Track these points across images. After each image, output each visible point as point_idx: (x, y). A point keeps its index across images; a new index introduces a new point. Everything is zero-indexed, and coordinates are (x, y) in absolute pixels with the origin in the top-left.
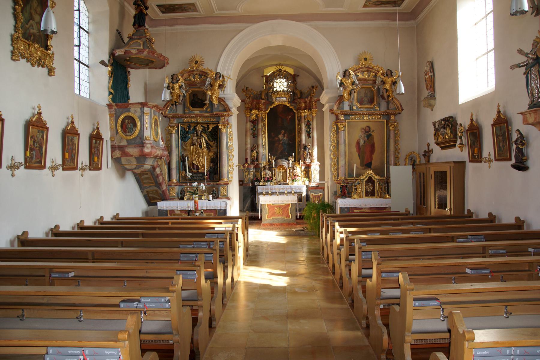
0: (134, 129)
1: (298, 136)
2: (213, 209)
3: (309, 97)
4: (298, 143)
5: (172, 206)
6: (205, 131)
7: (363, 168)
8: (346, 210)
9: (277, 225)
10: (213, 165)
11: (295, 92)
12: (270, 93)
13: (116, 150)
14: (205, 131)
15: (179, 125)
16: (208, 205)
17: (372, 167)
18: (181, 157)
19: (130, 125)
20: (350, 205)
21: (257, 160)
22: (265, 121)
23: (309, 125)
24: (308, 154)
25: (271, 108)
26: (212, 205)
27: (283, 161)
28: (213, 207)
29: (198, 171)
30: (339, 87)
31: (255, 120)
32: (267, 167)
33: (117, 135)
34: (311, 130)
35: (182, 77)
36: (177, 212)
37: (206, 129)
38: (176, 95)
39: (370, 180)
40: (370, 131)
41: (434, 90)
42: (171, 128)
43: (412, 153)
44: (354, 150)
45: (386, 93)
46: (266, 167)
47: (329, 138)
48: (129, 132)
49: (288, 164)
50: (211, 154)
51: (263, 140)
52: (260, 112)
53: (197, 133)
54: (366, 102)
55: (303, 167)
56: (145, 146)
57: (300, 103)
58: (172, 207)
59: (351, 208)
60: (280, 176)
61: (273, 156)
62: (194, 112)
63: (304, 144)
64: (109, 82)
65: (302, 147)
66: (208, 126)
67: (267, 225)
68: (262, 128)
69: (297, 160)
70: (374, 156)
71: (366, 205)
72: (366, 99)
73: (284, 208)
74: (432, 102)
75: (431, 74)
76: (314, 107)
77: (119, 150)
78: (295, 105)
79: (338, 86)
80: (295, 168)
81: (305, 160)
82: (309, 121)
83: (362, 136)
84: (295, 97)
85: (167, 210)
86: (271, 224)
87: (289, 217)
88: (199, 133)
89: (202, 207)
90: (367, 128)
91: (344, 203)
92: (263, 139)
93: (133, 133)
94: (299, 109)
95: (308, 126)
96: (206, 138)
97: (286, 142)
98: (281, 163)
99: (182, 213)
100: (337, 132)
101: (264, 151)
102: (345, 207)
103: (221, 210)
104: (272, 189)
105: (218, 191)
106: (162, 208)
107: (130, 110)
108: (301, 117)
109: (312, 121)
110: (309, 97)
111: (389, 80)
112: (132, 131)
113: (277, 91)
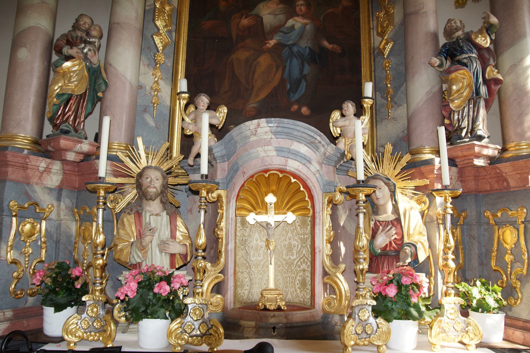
46: (145, 182)
61: (210, 94)
97: (305, 44)
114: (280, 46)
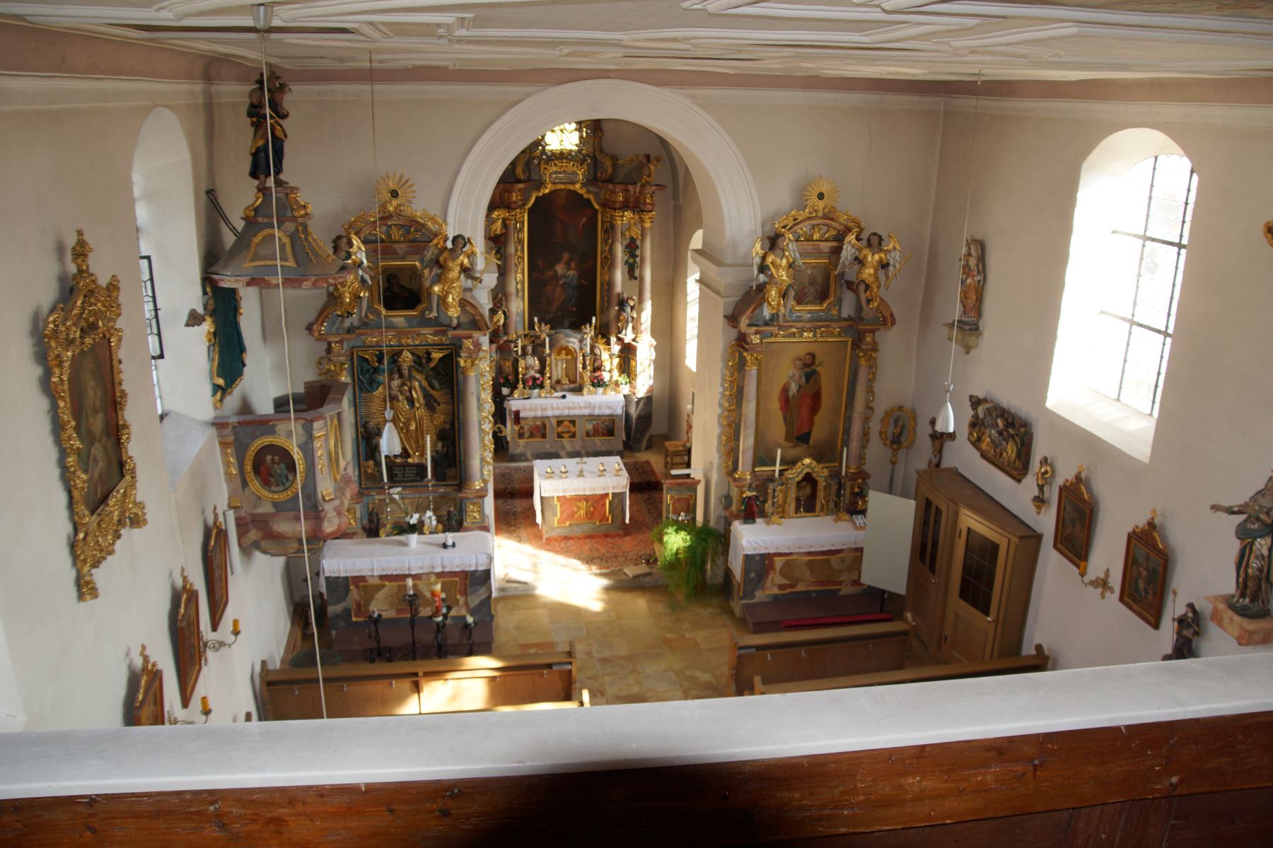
0: (291, 477)
1: (603, 267)
2: (458, 570)
3: (639, 185)
4: (601, 284)
5: (358, 566)
6: (421, 364)
7: (791, 444)
8: (757, 558)
9: (579, 539)
10: (443, 446)
11: (599, 158)
12: (534, 158)
13: (248, 531)
14: (421, 364)
15: (352, 354)
16: (446, 563)
17: (811, 442)
18: (362, 430)
19: (280, 468)
20: (766, 548)
21: (506, 333)
22: (521, 230)
23: (632, 248)
24: (630, 319)
25: (537, 198)
26: (457, 562)
27: (567, 336)
28: (457, 566)
29: (406, 462)
30: (758, 275)
31: (500, 236)
32: (530, 348)
33: (247, 489)
34: (638, 260)
35: (357, 234)
36: (372, 581)
37: (424, 361)
38: (350, 293)
39: (809, 479)
40: (813, 364)
41: (979, 314)
42: (335, 366)
43: (900, 408)
44: (775, 405)
45: (865, 292)
47: (720, 376)
48: (277, 485)
49: (581, 341)
50: (440, 418)
51: (519, 278)
52: (514, 213)
53: (400, 371)
54: (811, 298)
55: (616, 348)
56: (324, 519)
57: (613, 192)
58: (359, 571)
59: (769, 554)
60: (559, 368)
62: (391, 319)
63: (619, 294)
64: (211, 360)
65: (615, 301)
66: (429, 354)
67: (556, 540)
68: (517, 251)
69: (604, 333)
70: (817, 419)
71: (800, 548)
72: (812, 291)
73: (595, 501)
74: (972, 340)
75: (979, 278)
76: (648, 207)
77: (256, 528)
78: (597, 190)
79: (756, 272)
80: (597, 351)
81: (620, 333)
82: (633, 240)
83: (794, 375)
84: (599, 175)
85: (347, 578)
86: (566, 538)
87: (608, 520)
88: (407, 371)
89: (433, 567)
90: (808, 357)
91: (754, 544)
92: (518, 275)
93: (287, 485)
94: (607, 205)
95: (631, 250)
96: (424, 383)
97: (574, 282)
98: (563, 342)
99: (383, 583)
100: (741, 365)
101: (518, 306)
102: (756, 552)
103: (476, 571)
104: (546, 409)
105: (461, 511)
106: (334, 572)
107: (277, 428)
108: (613, 227)
109: (643, 240)
110: (639, 185)
111: (873, 258)
112: (284, 481)
113: (553, 153)
114: (564, 283)
